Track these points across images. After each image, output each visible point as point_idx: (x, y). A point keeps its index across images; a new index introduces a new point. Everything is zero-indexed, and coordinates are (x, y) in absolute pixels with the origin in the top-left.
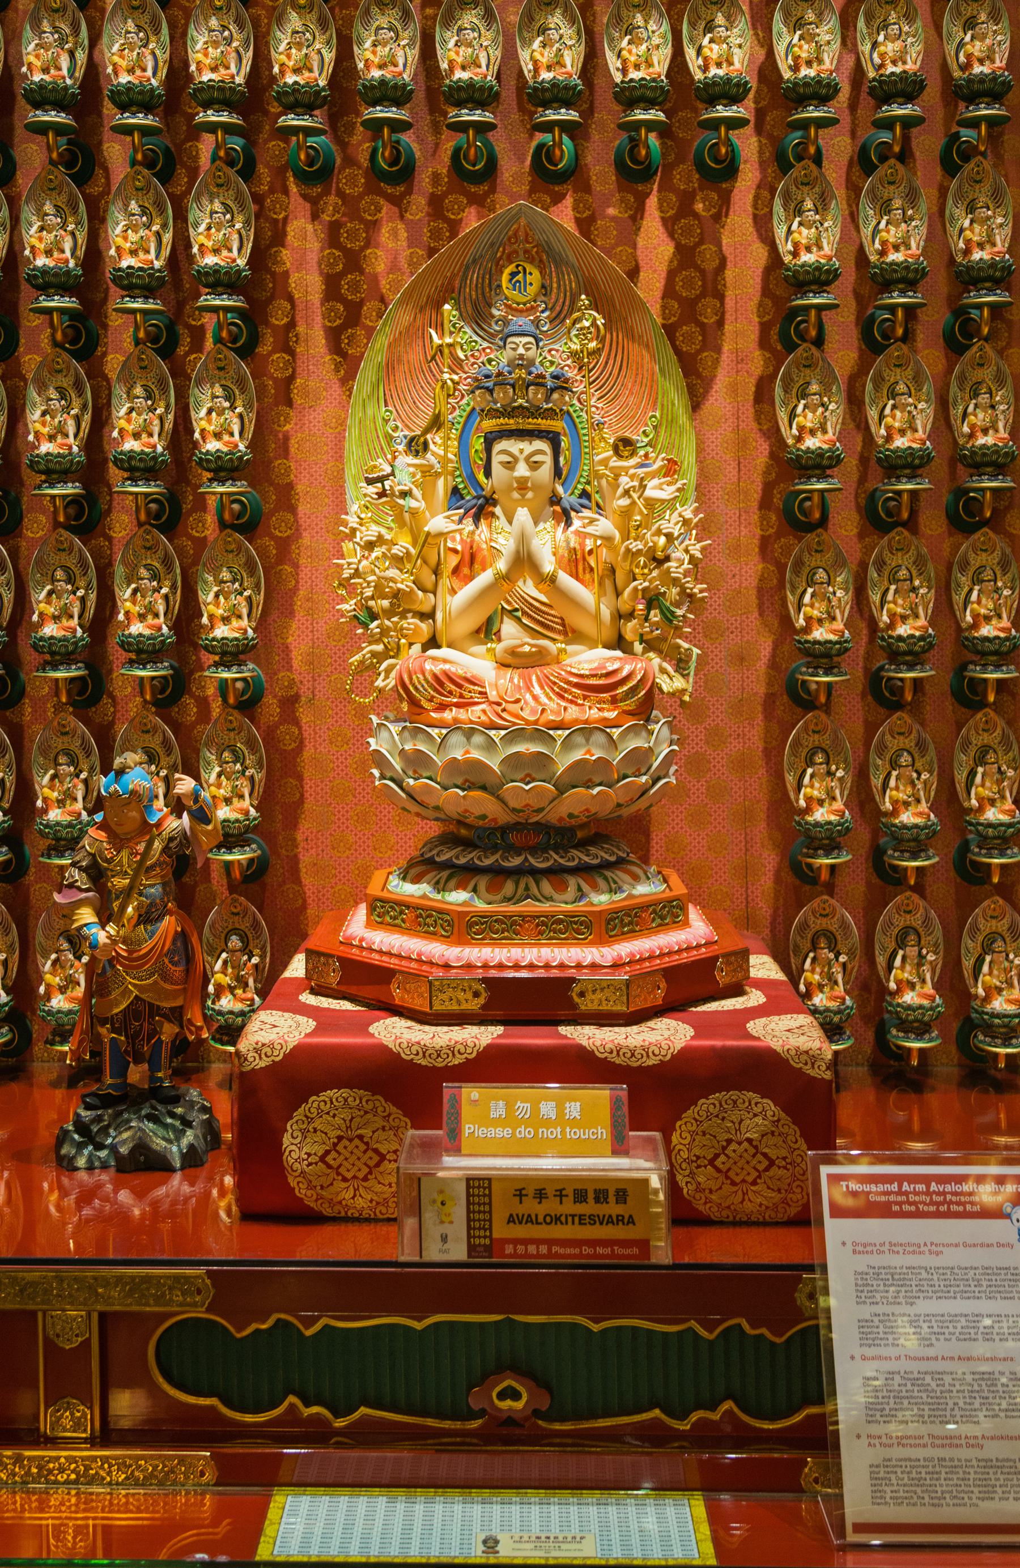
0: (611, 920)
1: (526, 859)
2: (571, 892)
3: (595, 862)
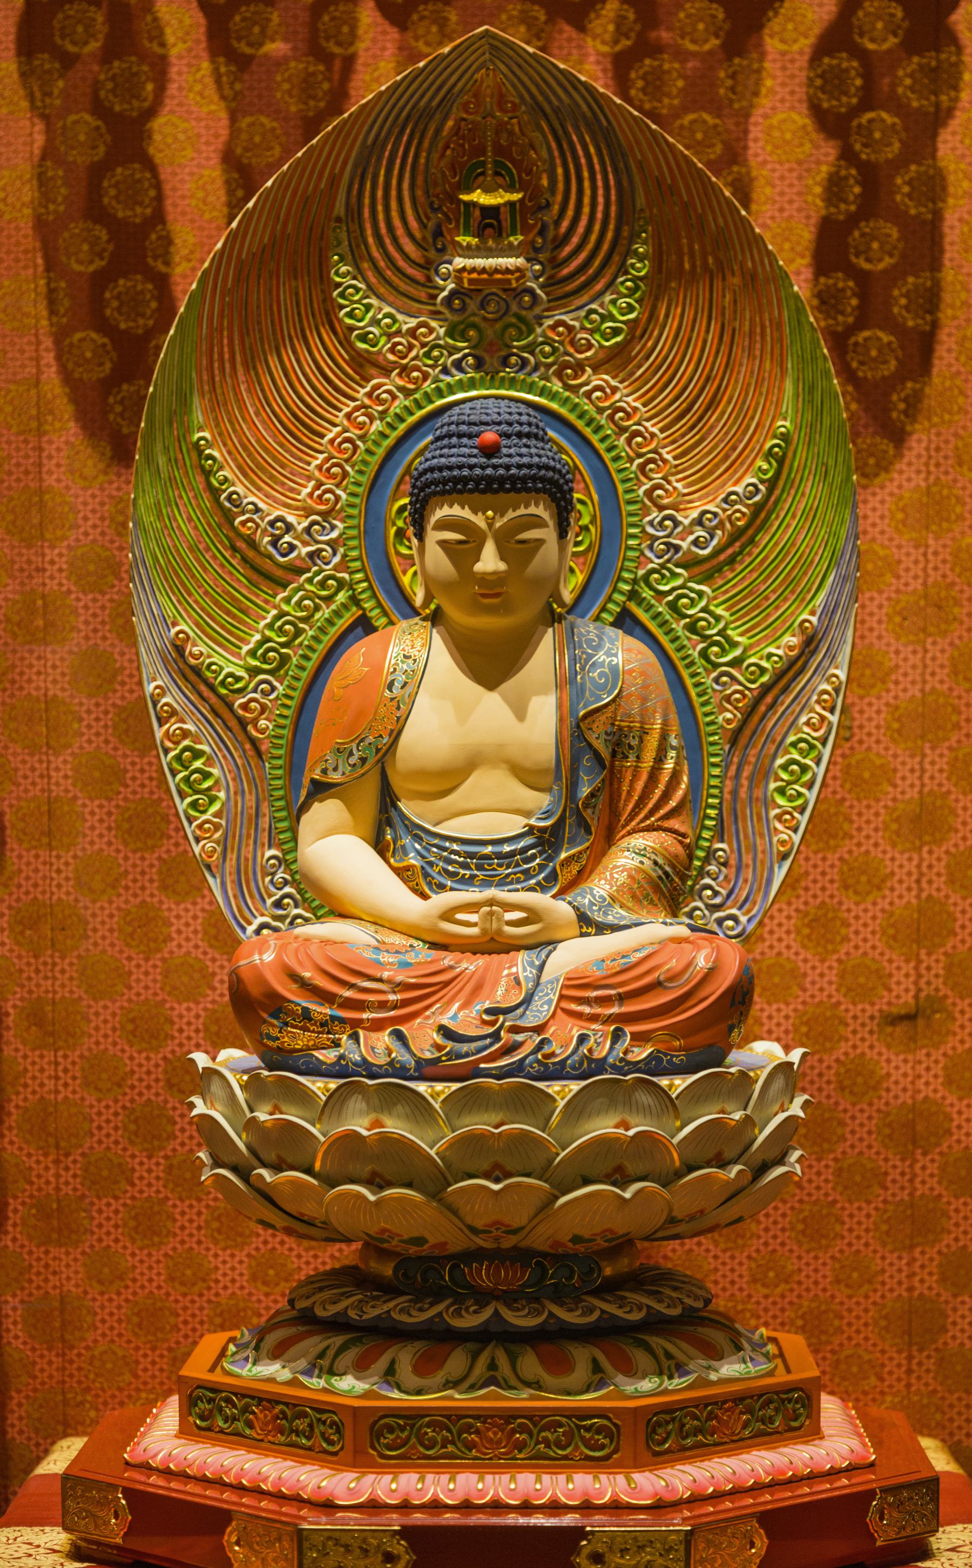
0: (658, 1424)
1: (496, 1312)
2: (581, 1373)
3: (636, 1316)
